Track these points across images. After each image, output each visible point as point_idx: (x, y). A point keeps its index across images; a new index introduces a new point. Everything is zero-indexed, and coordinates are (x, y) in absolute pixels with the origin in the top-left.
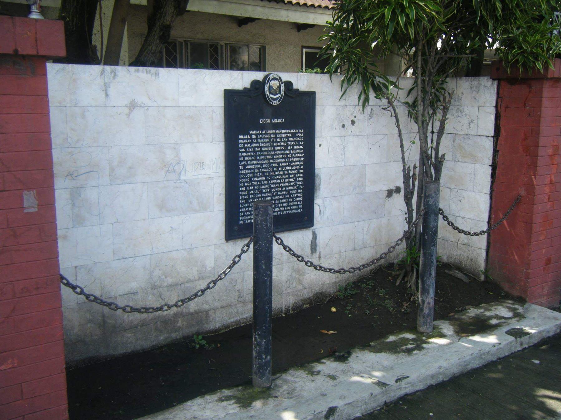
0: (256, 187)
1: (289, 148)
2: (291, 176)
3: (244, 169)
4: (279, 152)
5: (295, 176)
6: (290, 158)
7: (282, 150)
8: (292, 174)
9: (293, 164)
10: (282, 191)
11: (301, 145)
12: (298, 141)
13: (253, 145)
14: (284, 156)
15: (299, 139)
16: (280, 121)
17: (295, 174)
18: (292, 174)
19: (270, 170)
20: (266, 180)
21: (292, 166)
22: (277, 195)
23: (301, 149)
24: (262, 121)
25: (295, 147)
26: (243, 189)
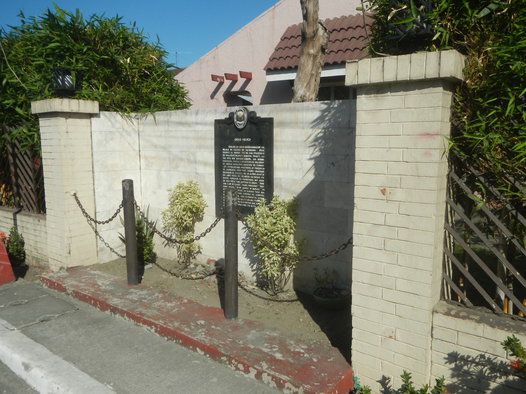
0: (233, 184)
1: (254, 159)
2: (255, 180)
3: (226, 171)
4: (247, 162)
5: (259, 181)
6: (254, 167)
7: (249, 160)
8: (256, 179)
9: (257, 171)
10: (249, 190)
11: (263, 158)
12: (261, 155)
13: (231, 155)
14: (250, 165)
15: (261, 153)
16: (248, 140)
17: (259, 179)
18: (256, 179)
20: (239, 180)
21: (256, 173)
22: (246, 192)
23: (263, 161)
24: (236, 140)
25: (258, 159)
26: (225, 184)
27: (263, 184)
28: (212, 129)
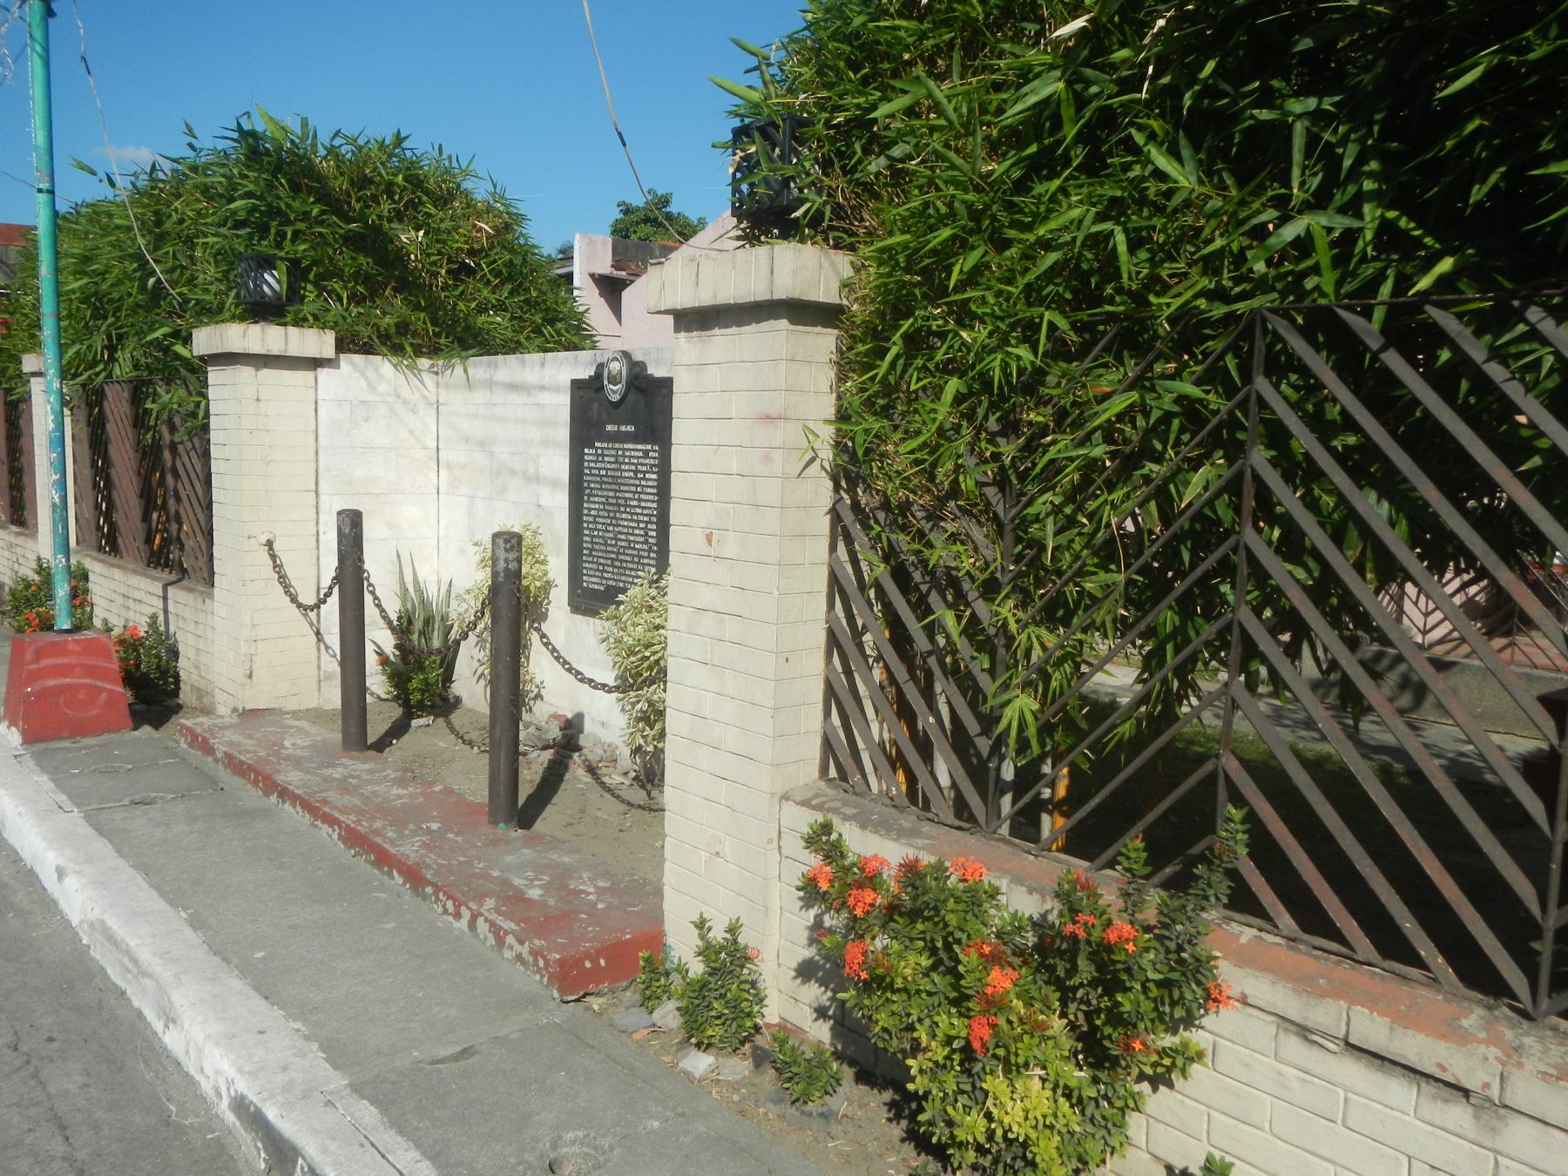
4: (627, 481)
7: (630, 478)
9: (643, 504)
10: (629, 548)
12: (651, 466)
13: (599, 465)
15: (652, 462)
17: (647, 523)
19: (616, 508)
21: (643, 508)
24: (609, 428)
27: (654, 534)
28: (565, 400)
